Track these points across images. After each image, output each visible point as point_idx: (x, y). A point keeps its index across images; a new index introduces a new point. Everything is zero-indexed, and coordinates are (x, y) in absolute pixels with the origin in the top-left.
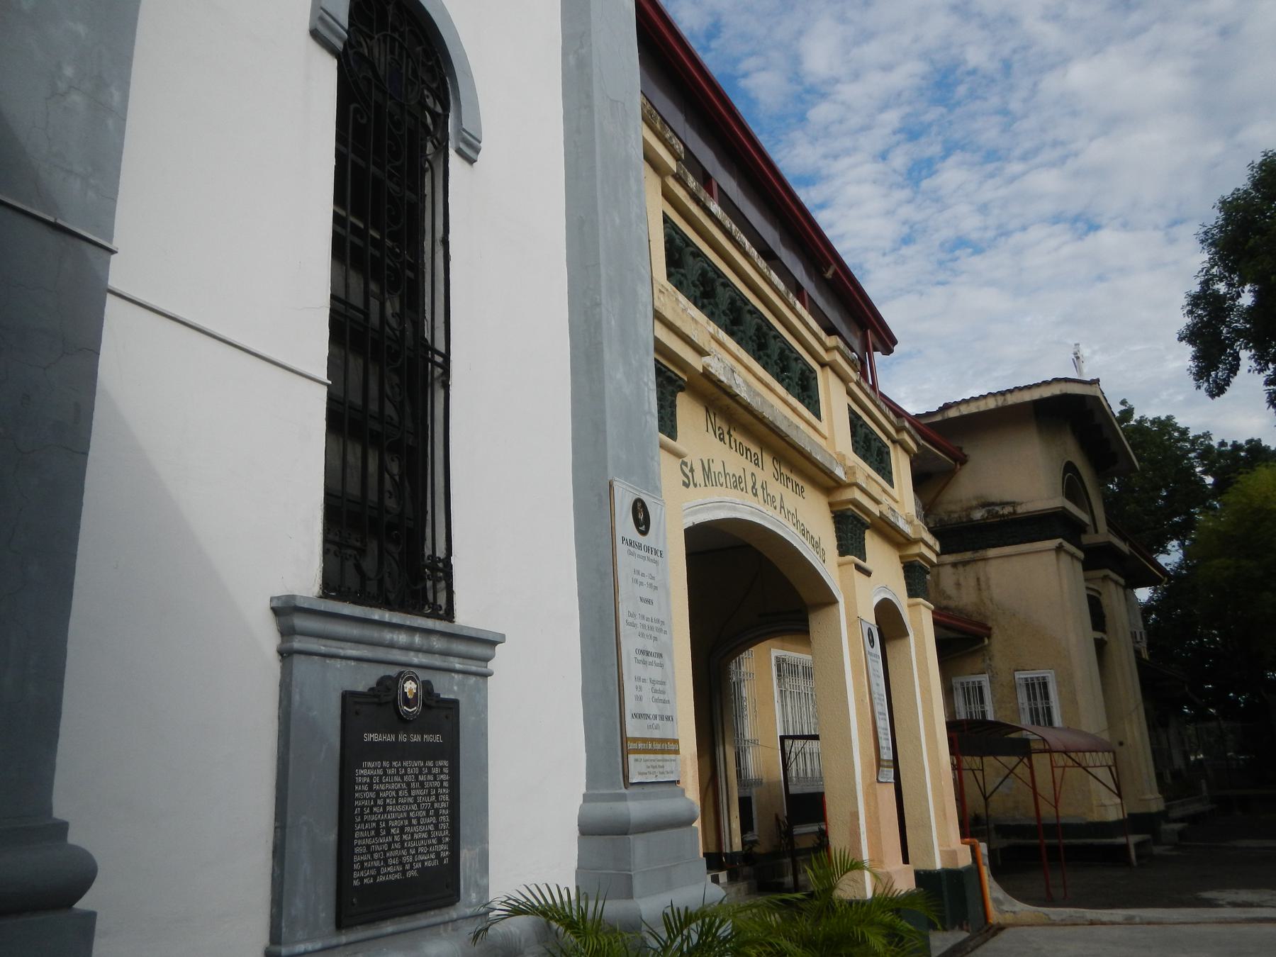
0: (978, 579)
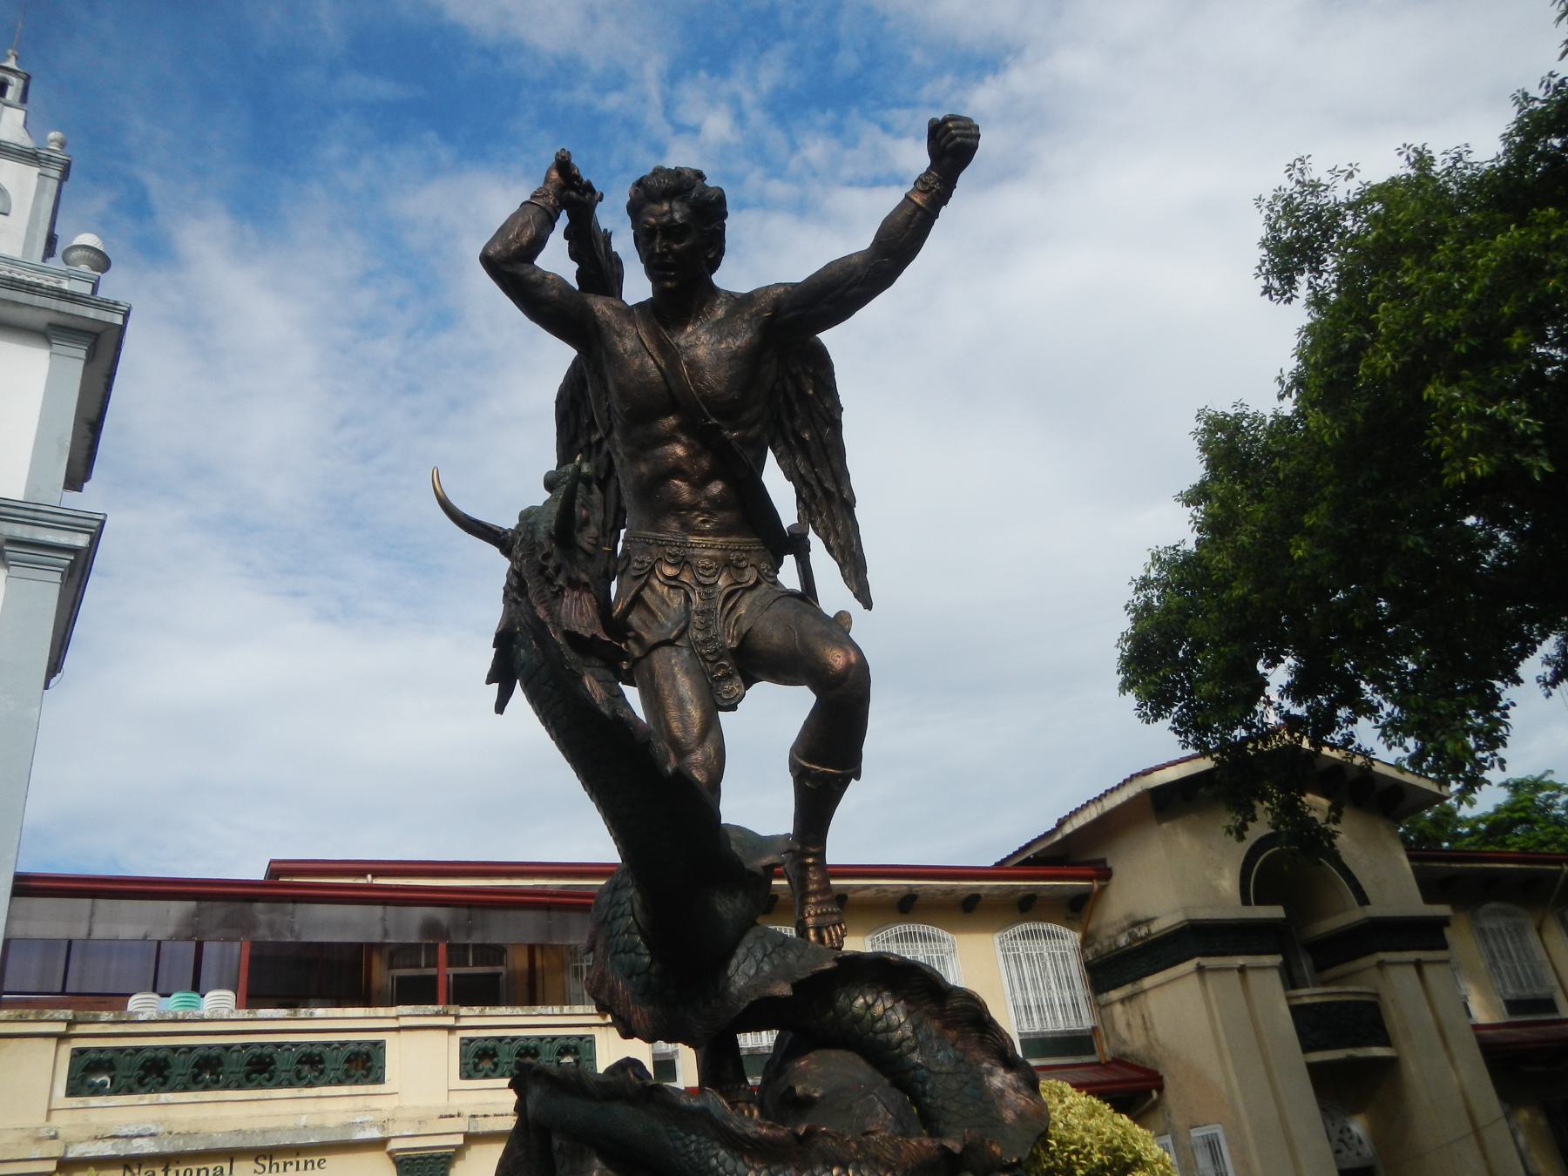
0: (1143, 1017)
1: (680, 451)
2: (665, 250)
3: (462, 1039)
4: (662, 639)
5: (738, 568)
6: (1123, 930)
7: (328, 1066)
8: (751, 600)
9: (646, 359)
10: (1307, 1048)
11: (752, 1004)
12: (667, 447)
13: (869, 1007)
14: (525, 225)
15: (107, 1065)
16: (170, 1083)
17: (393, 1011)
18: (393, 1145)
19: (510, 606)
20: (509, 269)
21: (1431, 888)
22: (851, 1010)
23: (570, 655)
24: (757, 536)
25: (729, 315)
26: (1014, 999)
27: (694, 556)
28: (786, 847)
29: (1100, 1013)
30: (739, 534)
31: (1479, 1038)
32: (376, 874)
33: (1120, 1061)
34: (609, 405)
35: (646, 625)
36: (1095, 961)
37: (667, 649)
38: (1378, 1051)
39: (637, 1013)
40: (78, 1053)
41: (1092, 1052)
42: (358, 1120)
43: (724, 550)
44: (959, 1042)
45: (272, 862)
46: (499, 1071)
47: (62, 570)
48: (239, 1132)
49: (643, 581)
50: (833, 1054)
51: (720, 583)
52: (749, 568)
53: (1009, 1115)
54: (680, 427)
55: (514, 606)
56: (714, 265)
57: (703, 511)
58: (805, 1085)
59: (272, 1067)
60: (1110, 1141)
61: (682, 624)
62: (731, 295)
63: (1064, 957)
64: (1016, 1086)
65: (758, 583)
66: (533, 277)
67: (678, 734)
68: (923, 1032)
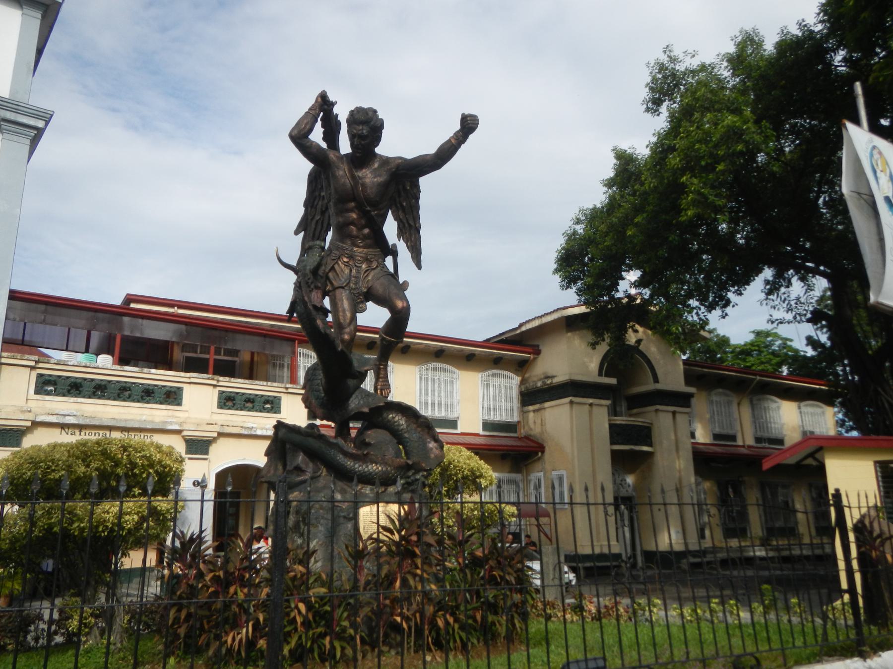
1: (354, 216)
7: (156, 395)
10: (613, 442)
13: (393, 418)
14: (306, 124)
16: (82, 394)
17: (188, 375)
18: (185, 433)
21: (690, 378)
23: (314, 313)
25: (380, 166)
26: (483, 404)
31: (693, 448)
32: (180, 307)
33: (527, 438)
37: (341, 289)
38: (645, 448)
40: (40, 376)
41: (516, 432)
42: (169, 420)
45: (128, 295)
46: (235, 407)
48: (114, 419)
50: (380, 431)
53: (432, 456)
54: (356, 207)
56: (376, 146)
57: (360, 239)
60: (472, 468)
62: (381, 156)
63: (511, 388)
67: (342, 321)
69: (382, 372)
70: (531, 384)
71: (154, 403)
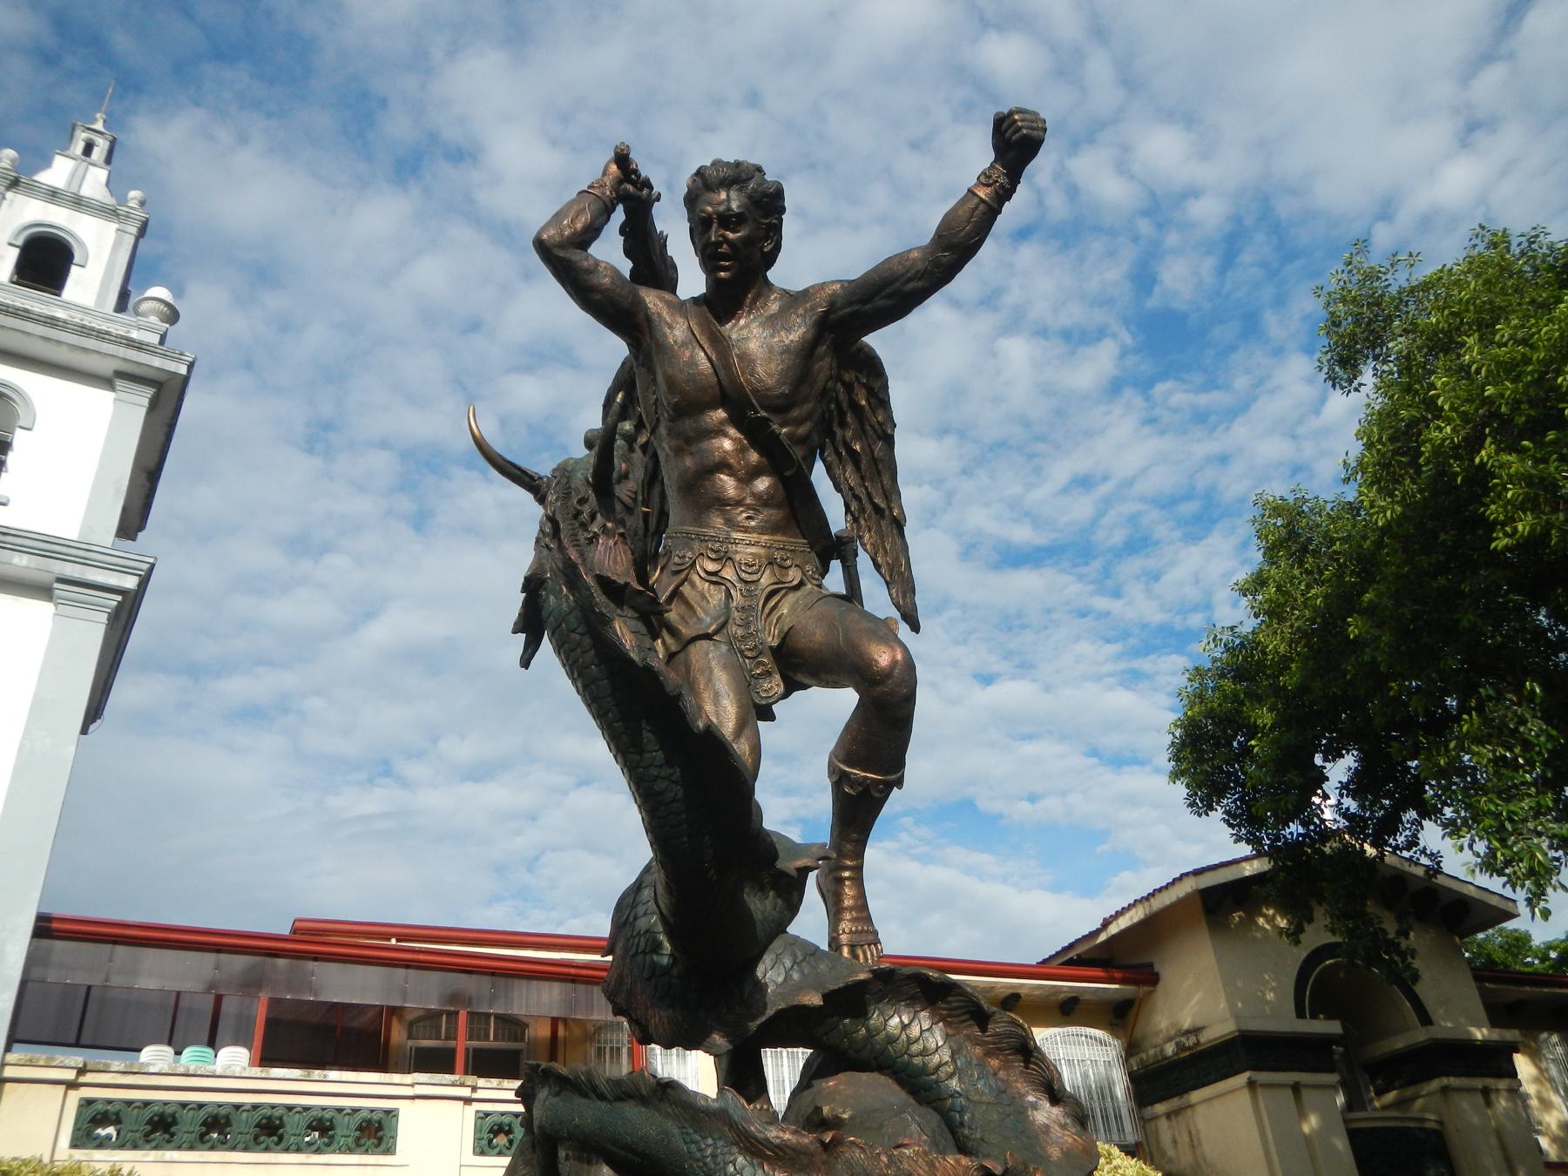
2: (721, 239)
3: (477, 1112)
4: (700, 633)
5: (781, 567)
6: (1170, 1040)
7: (339, 1131)
8: (794, 599)
9: (696, 351)
11: (780, 1013)
12: (714, 441)
13: (904, 1027)
14: (581, 211)
15: (114, 1117)
19: (541, 552)
20: (561, 254)
22: (885, 1029)
23: (600, 598)
24: (804, 538)
25: (783, 311)
27: (737, 552)
28: (822, 854)
29: (1144, 1127)
30: (784, 534)
34: (657, 399)
35: (686, 621)
36: (1140, 1071)
37: (704, 643)
39: (655, 1017)
40: (88, 1103)
43: (769, 548)
44: (1001, 1072)
47: (109, 610)
49: (683, 576)
50: (865, 1077)
51: (762, 580)
52: (793, 569)
53: (1055, 1153)
55: (545, 552)
56: (770, 259)
57: (749, 507)
58: (832, 1106)
59: (281, 1131)
61: (722, 620)
64: (1063, 1122)
65: (801, 584)
66: (585, 264)
68: (963, 1060)
69: (849, 891)
70: (1152, 1052)
71: (334, 1152)
